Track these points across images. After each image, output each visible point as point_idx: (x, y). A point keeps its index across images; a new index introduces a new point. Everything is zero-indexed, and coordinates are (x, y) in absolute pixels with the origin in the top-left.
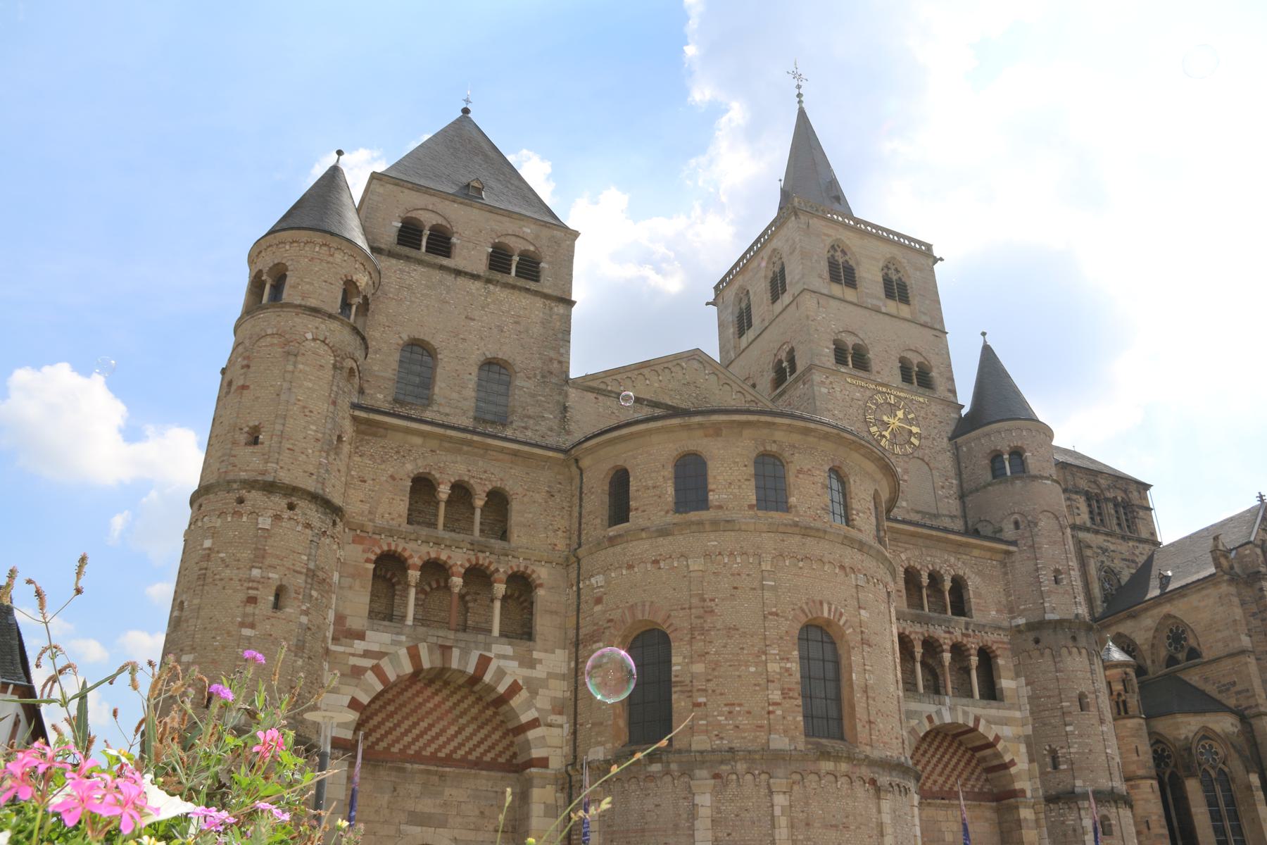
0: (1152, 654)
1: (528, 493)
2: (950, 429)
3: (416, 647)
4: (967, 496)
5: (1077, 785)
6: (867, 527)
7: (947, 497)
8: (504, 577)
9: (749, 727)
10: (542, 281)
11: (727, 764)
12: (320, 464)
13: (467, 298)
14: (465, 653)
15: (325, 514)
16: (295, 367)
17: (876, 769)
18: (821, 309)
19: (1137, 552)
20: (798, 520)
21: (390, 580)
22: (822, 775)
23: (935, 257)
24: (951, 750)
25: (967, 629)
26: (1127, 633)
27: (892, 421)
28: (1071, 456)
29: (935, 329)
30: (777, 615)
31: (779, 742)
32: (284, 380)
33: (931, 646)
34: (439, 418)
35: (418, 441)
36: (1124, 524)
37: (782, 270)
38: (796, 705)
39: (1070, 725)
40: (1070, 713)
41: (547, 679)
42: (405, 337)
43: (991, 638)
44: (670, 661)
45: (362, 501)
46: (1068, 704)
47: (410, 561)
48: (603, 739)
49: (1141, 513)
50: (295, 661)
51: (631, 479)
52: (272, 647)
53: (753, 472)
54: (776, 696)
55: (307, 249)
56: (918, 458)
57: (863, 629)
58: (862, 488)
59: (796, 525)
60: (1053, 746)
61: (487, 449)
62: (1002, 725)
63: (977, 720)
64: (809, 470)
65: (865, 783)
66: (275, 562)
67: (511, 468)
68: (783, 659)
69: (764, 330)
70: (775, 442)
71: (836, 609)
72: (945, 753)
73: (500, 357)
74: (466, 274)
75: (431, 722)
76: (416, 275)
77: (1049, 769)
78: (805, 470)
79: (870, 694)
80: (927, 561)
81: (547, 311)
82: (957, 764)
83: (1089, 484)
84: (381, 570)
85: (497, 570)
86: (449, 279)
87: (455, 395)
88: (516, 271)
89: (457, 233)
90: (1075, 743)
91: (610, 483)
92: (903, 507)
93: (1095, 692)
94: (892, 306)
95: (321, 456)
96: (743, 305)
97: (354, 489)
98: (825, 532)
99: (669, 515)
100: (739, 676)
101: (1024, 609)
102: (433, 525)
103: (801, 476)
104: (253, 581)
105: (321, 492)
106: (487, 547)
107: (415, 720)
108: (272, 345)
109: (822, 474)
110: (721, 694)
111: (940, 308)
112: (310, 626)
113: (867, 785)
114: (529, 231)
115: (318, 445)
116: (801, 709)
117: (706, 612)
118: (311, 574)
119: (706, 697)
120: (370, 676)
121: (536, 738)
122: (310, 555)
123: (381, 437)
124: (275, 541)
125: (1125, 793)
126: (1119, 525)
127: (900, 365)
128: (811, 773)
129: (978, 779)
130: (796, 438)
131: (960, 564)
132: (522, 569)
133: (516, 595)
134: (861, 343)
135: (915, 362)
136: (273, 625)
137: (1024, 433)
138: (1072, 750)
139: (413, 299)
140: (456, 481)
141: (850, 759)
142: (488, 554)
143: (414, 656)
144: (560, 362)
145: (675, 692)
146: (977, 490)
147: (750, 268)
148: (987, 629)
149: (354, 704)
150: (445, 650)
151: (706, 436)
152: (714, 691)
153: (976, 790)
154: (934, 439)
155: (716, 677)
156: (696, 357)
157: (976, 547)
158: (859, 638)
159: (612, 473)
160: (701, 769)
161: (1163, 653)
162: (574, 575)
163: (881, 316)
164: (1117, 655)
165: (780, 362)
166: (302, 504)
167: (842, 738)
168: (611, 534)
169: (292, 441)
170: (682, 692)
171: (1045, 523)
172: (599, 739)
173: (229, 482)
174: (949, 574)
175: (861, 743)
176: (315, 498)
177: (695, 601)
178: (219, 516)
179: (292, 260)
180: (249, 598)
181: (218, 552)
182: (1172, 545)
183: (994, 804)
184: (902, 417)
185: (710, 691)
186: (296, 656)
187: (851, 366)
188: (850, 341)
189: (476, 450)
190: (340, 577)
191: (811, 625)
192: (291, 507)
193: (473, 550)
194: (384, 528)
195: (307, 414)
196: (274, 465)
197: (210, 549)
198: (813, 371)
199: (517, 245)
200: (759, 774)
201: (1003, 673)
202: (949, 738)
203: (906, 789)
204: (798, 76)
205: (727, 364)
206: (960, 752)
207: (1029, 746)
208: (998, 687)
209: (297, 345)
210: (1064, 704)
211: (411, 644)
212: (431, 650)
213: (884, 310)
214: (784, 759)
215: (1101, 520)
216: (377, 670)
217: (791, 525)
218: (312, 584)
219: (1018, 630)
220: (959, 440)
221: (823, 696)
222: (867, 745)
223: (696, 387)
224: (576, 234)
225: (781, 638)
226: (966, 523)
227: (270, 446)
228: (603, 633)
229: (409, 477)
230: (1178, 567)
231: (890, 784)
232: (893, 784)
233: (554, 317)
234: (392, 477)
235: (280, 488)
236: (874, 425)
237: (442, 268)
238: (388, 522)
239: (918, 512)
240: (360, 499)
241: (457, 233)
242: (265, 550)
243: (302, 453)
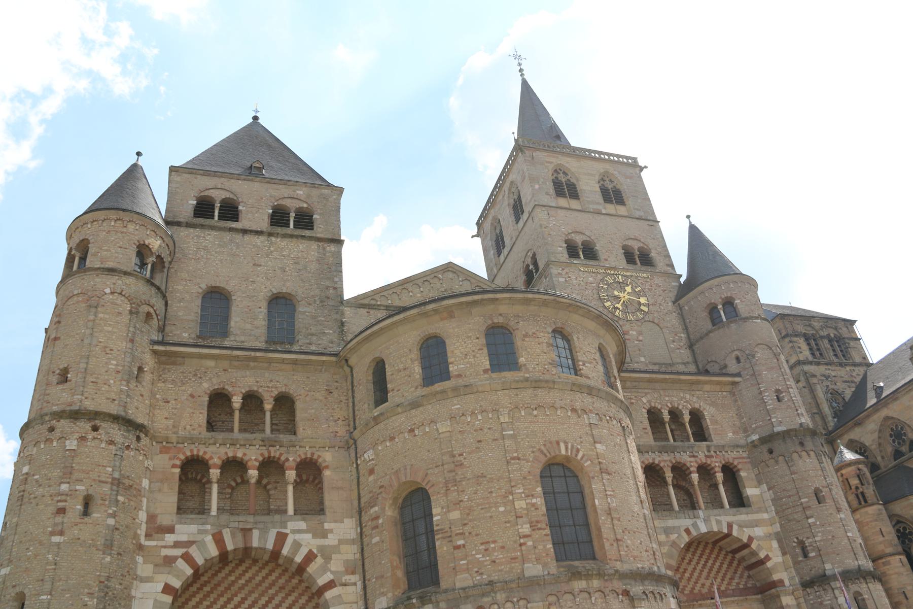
0: (881, 451)
1: (309, 393)
2: (673, 295)
3: (220, 533)
4: (695, 344)
5: (827, 568)
6: (594, 374)
7: (678, 349)
8: (294, 465)
9: (504, 560)
10: (315, 229)
11: (487, 596)
12: (121, 391)
13: (253, 250)
14: (264, 532)
15: (128, 431)
16: (96, 316)
17: (628, 581)
18: (551, 218)
19: (854, 374)
20: (528, 375)
21: (200, 480)
22: (576, 593)
23: (641, 166)
24: (713, 556)
25: (709, 451)
26: (857, 438)
27: (622, 295)
28: (787, 310)
29: (649, 220)
31: (533, 570)
32: (87, 328)
33: (680, 470)
34: (235, 344)
35: (211, 363)
36: (840, 354)
37: (519, 197)
38: (545, 535)
39: (812, 517)
40: (810, 507)
41: (339, 545)
42: (204, 286)
43: (731, 456)
44: (431, 515)
45: (166, 418)
46: (806, 500)
47: (211, 462)
48: (385, 590)
49: (852, 344)
50: (103, 558)
51: (386, 366)
52: (80, 549)
53: (485, 342)
54: (526, 529)
55: (104, 224)
56: (649, 321)
57: (600, 460)
58: (586, 343)
59: (527, 380)
60: (800, 538)
61: (270, 363)
62: (753, 527)
63: (730, 526)
64: (534, 333)
65: (618, 595)
66: (82, 476)
67: (293, 375)
68: (529, 496)
69: (513, 246)
70: (501, 315)
71: (572, 446)
72: (708, 559)
73: (284, 291)
74: (251, 231)
75: (243, 596)
76: (209, 238)
77: (801, 559)
78: (531, 334)
79: (615, 515)
80: (664, 401)
81: (321, 251)
82: (721, 566)
83: (806, 327)
84: (192, 473)
85: (287, 460)
86: (238, 237)
87: (249, 326)
88: (294, 225)
89: (242, 202)
90: (819, 532)
91: (373, 373)
92: (642, 362)
93: (828, 485)
94: (610, 208)
95: (121, 385)
96: (498, 231)
97: (159, 409)
98: (554, 382)
99: (418, 390)
100: (491, 517)
101: (756, 427)
102: (232, 430)
103: (527, 339)
104: (62, 495)
105: (123, 414)
106: (276, 441)
107: (230, 596)
108: (78, 302)
109: (546, 335)
110: (477, 535)
111: (651, 204)
112: (118, 527)
113: (621, 596)
114: (301, 193)
115: (119, 376)
116: (550, 538)
117: (456, 466)
118: (117, 483)
119: (464, 539)
120: (181, 563)
121: (333, 597)
122: (115, 466)
123: (180, 364)
124: (81, 459)
125: (872, 569)
126: (836, 355)
127: (623, 251)
128: (566, 593)
129: (741, 577)
130: (518, 309)
131: (695, 399)
132: (309, 456)
133: (311, 479)
134: (588, 239)
135: (636, 247)
136: (81, 530)
137: (732, 286)
138: (817, 539)
139: (209, 256)
140: (247, 392)
141: (600, 575)
142: (278, 447)
143: (219, 540)
144: (335, 288)
145: (438, 539)
146: (702, 338)
147: (498, 201)
148: (726, 449)
149: (167, 589)
150: (246, 532)
151: (442, 319)
152: (470, 533)
153: (741, 586)
154: (660, 304)
155: (470, 521)
156: (450, 269)
157: (706, 383)
158: (598, 468)
159: (373, 364)
160: (465, 603)
161: (890, 449)
162: (353, 455)
163: (602, 216)
164: (849, 456)
165: (528, 266)
166: (104, 425)
167: (594, 558)
168: (376, 414)
169: (96, 376)
170: (444, 538)
171: (761, 354)
172: (382, 590)
173: (42, 416)
174: (687, 408)
175: (610, 559)
176: (116, 419)
177: (446, 458)
178: (35, 445)
179: (93, 235)
180: (59, 509)
181: (33, 475)
182: (880, 362)
183: (759, 596)
184: (630, 291)
185: (467, 534)
186: (104, 554)
187: (582, 258)
188: (579, 239)
189: (261, 364)
190: (151, 482)
191: (553, 464)
192: (95, 429)
193: (265, 446)
194: (186, 437)
195: (108, 352)
196: (79, 397)
197: (27, 474)
198: (551, 266)
200: (518, 601)
201: (746, 483)
202: (710, 546)
203: (661, 595)
204: (517, 57)
205: (493, 277)
206: (721, 557)
207: (780, 542)
208: (744, 495)
209: (97, 299)
210: (802, 500)
211: (215, 531)
212: (233, 535)
213: (604, 211)
214: (538, 584)
215: (821, 354)
216: (187, 558)
217: (522, 382)
218: (118, 491)
219: (753, 445)
220: (682, 302)
221: (571, 523)
222: (617, 560)
224: (340, 190)
225: (525, 478)
226: (697, 366)
227: (76, 382)
228: (377, 498)
229: (206, 393)
230: (888, 378)
231: (644, 592)
232: (647, 592)
233: (327, 254)
234: (192, 396)
235: (84, 414)
236: (607, 301)
237: (231, 230)
238: (189, 432)
239: (655, 364)
240: (165, 416)
241: (242, 202)
242: (72, 467)
243: (105, 384)
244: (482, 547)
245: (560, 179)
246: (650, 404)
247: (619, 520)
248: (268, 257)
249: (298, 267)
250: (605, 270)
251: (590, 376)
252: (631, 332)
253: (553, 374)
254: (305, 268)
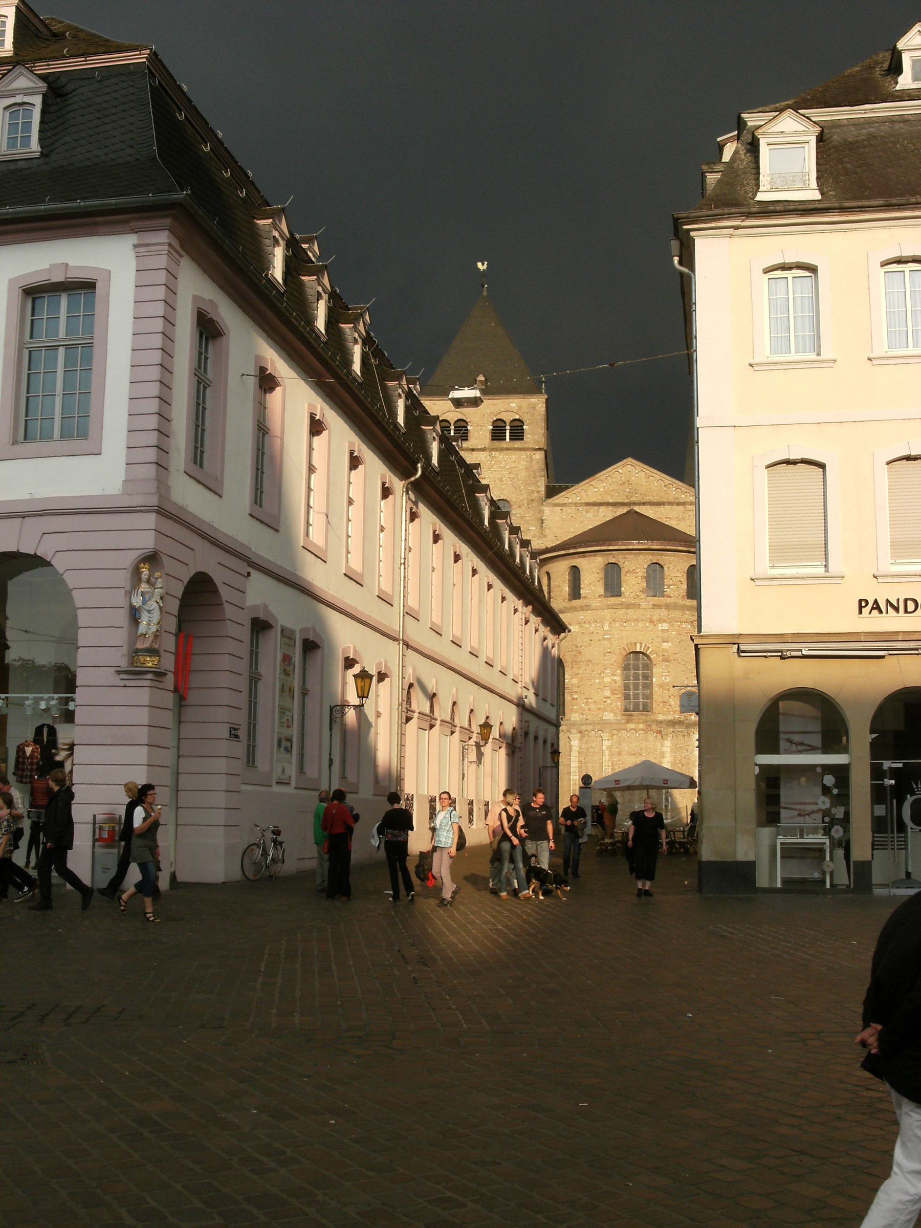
30: (610, 652)
31: (608, 716)
54: (608, 693)
71: (645, 645)
81: (528, 460)
103: (628, 575)
114: (514, 405)
199: (508, 417)
223: (629, 484)
244: (585, 701)
247: (668, 690)
248: (490, 470)
249: (512, 476)
251: (671, 595)
254: (517, 475)
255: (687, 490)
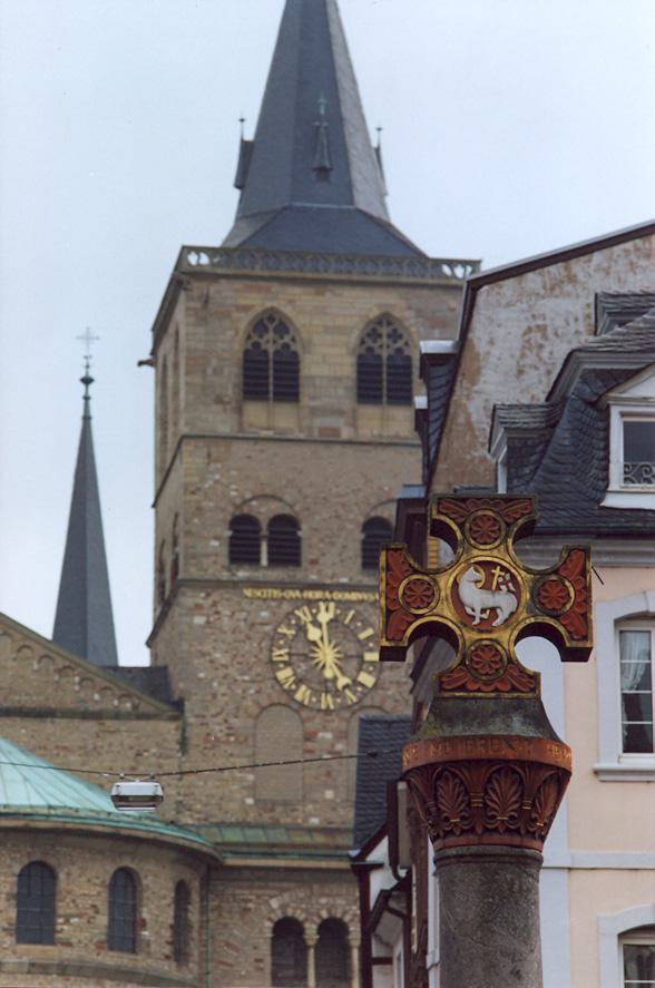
58: (83, 879)
92: (326, 801)
109: (9, 879)
134: (287, 511)
163: (338, 448)
245: (263, 347)
246: (284, 912)
250: (302, 591)
251: (74, 941)
252: (320, 735)
253: (5, 949)
255: (106, 684)
